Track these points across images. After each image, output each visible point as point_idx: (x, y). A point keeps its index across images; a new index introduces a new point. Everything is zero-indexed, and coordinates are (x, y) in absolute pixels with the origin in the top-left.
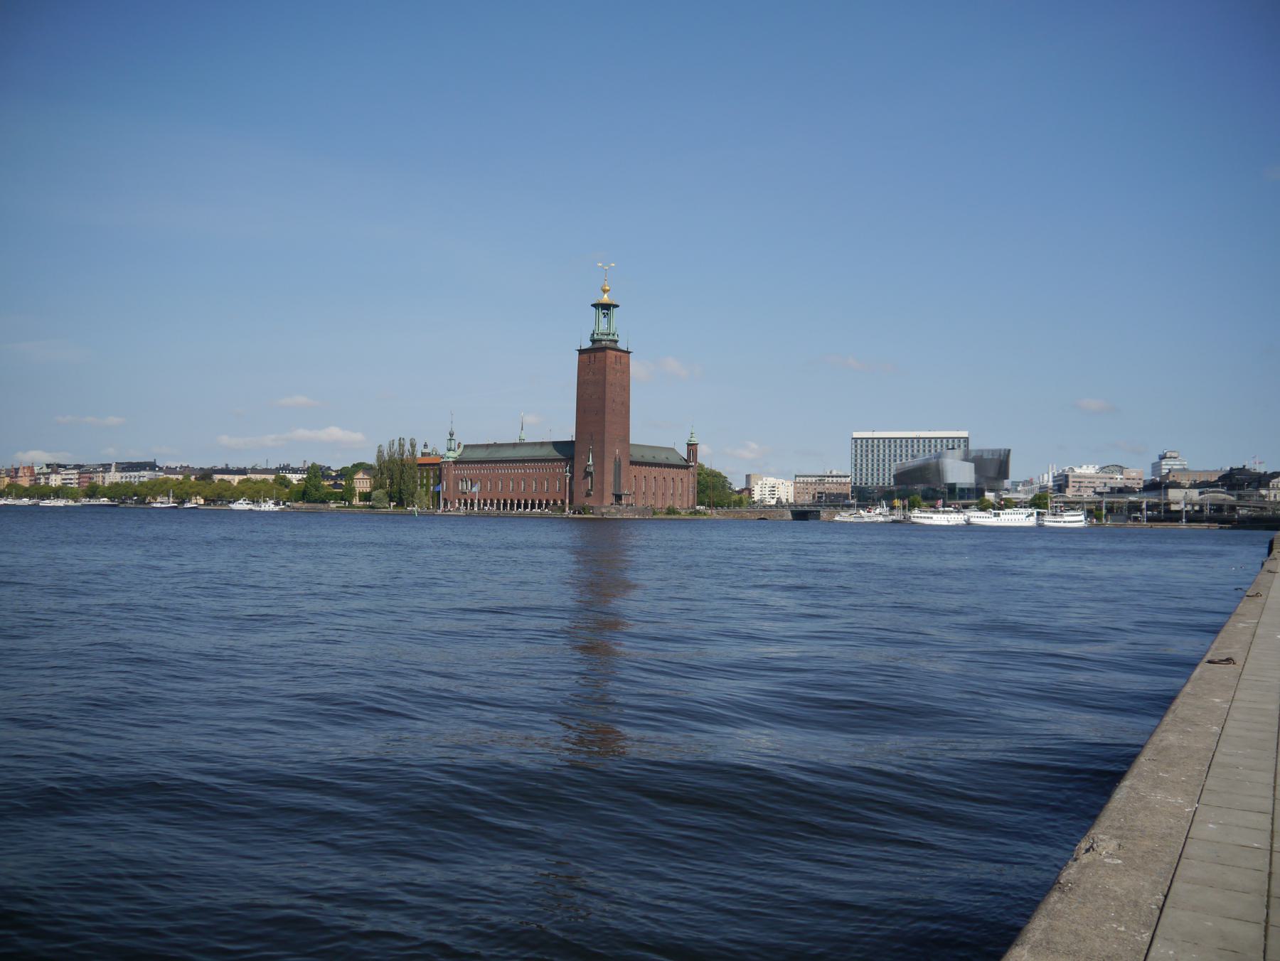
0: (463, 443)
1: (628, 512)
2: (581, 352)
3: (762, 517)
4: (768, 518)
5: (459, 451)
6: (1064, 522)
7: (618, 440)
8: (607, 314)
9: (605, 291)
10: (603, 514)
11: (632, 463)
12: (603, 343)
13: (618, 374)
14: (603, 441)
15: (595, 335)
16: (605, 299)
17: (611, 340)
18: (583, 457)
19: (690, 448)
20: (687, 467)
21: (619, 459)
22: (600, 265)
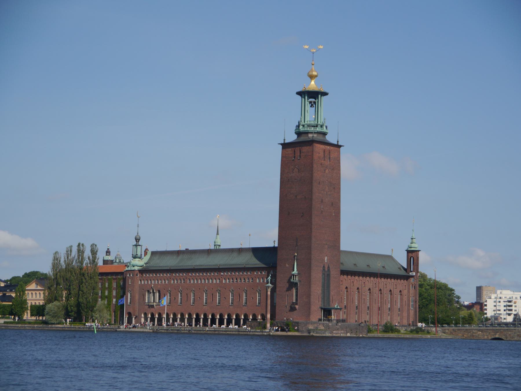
0: (151, 249)
1: (338, 329)
3: (497, 336)
4: (503, 337)
5: (146, 259)
7: (326, 246)
8: (315, 103)
9: (312, 77)
10: (309, 331)
11: (344, 273)
12: (310, 135)
13: (327, 171)
14: (309, 248)
15: (301, 127)
16: (313, 85)
17: (319, 133)
18: (287, 265)
19: (410, 255)
20: (407, 278)
21: (328, 267)
22: (306, 47)
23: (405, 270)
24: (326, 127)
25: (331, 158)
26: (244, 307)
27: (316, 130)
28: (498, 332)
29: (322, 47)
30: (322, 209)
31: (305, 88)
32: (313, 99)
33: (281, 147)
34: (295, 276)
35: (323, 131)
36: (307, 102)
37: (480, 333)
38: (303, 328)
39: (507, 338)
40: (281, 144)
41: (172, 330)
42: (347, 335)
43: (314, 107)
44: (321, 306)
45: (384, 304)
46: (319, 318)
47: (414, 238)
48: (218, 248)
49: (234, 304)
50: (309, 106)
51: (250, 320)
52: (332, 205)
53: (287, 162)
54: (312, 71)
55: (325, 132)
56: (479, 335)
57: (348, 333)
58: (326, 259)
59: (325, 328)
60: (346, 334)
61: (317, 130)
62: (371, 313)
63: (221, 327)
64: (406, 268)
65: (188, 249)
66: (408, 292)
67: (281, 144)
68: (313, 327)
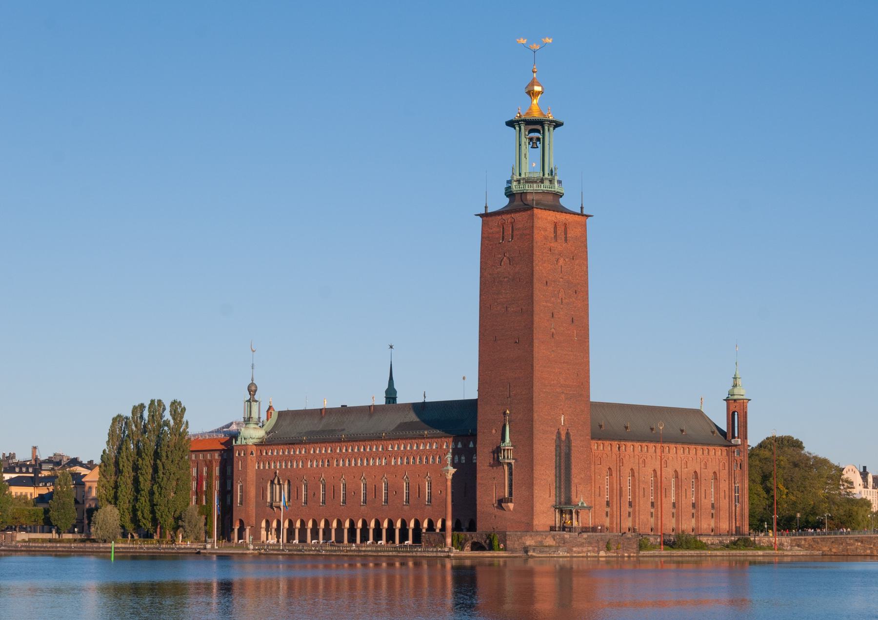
0: (279, 407)
1: (582, 545)
2: (485, 216)
7: (563, 396)
9: (531, 94)
10: (526, 550)
13: (561, 261)
14: (530, 400)
16: (536, 108)
21: (568, 434)
22: (523, 41)
24: (560, 182)
25: (568, 238)
26: (428, 507)
27: (539, 188)
29: (550, 41)
30: (553, 330)
31: (519, 113)
32: (536, 133)
33: (481, 219)
34: (506, 451)
35: (553, 189)
36: (524, 140)
37: (859, 544)
40: (481, 215)
42: (599, 554)
43: (537, 147)
45: (684, 497)
46: (551, 525)
47: (739, 378)
49: (410, 502)
50: (527, 146)
52: (573, 321)
53: (490, 247)
54: (533, 83)
55: (557, 192)
56: (857, 548)
57: (602, 550)
59: (556, 542)
60: (598, 552)
61: (542, 188)
62: (658, 514)
63: (377, 543)
64: (726, 431)
65: (346, 406)
66: (729, 475)
67: (481, 215)
68: (533, 541)
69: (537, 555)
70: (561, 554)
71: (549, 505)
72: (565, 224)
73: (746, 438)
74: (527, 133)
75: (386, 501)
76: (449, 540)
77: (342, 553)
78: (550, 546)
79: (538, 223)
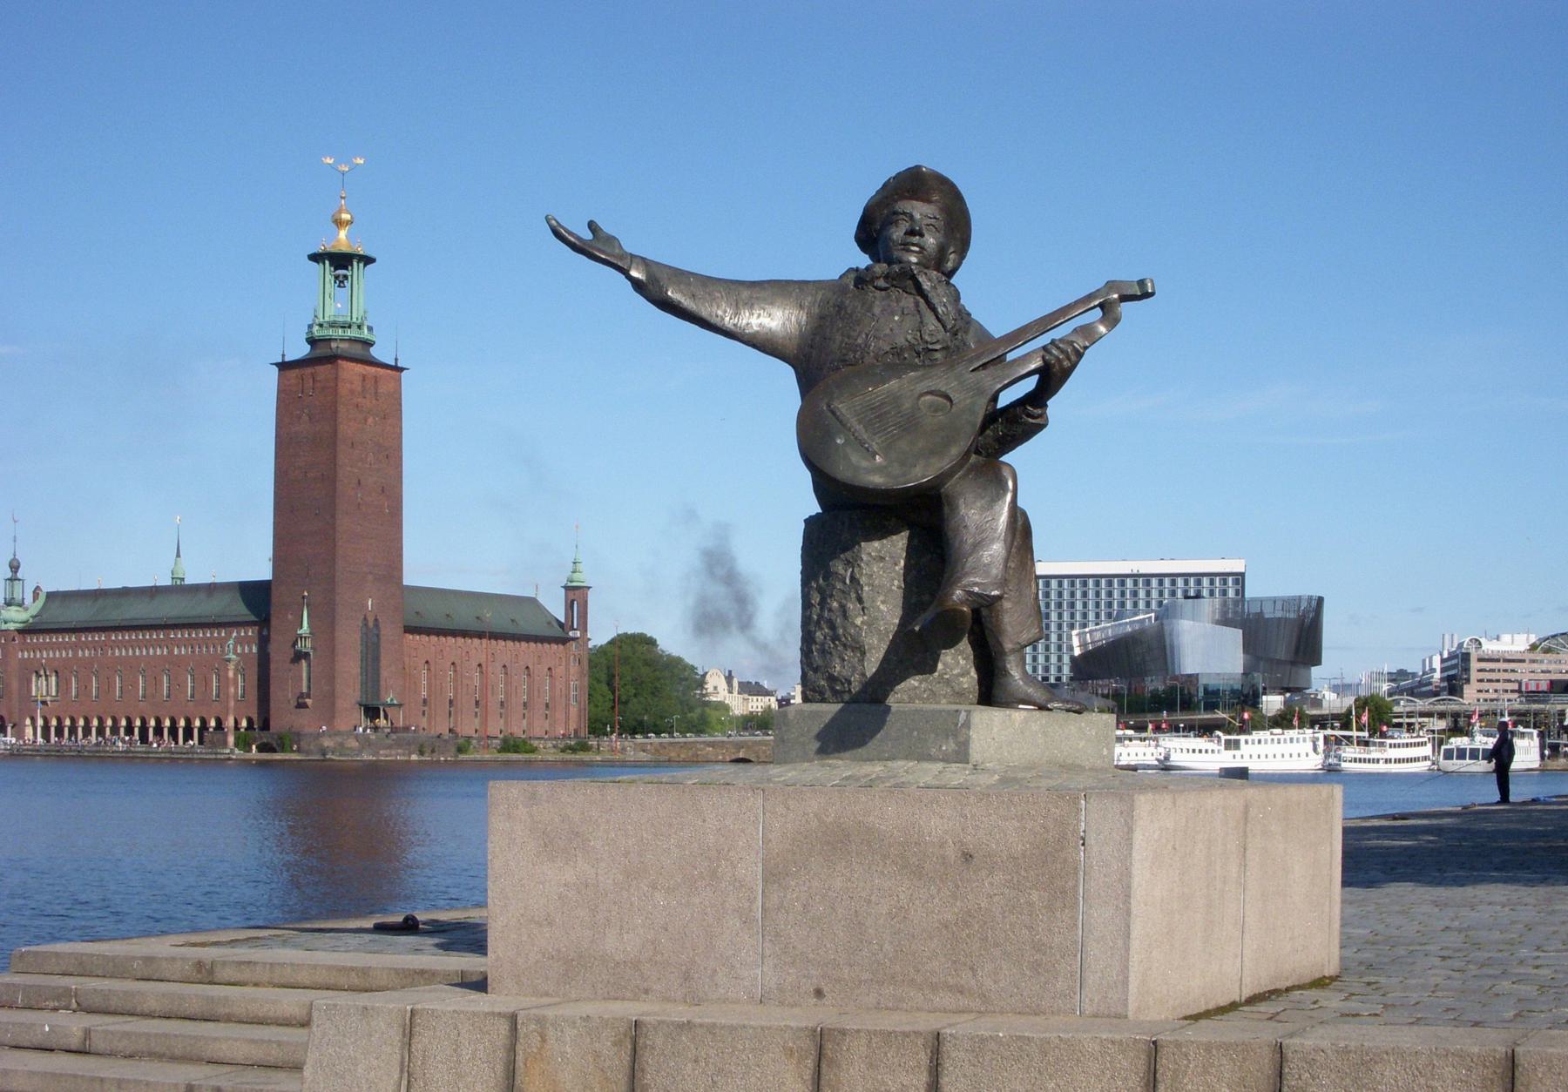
0: (48, 587)
1: (390, 747)
2: (283, 366)
3: (741, 755)
5: (34, 608)
6: (1387, 761)
7: (370, 577)
9: (339, 223)
11: (410, 630)
12: (334, 345)
13: (370, 420)
15: (316, 328)
17: (351, 340)
18: (290, 617)
19: (571, 594)
20: (564, 641)
21: (376, 620)
23: (561, 625)
24: (370, 329)
28: (743, 747)
31: (324, 245)
33: (277, 369)
37: (711, 749)
38: (309, 745)
39: (758, 757)
41: (46, 751)
42: (410, 757)
44: (359, 699)
48: (178, 583)
51: (211, 730)
54: (340, 212)
56: (707, 754)
58: (370, 603)
61: (349, 334)
69: (337, 758)
70: (365, 758)
71: (353, 701)
72: (376, 377)
73: (586, 631)
74: (332, 269)
75: (168, 696)
76: (231, 740)
77: (108, 754)
78: (351, 749)
79: (343, 375)
